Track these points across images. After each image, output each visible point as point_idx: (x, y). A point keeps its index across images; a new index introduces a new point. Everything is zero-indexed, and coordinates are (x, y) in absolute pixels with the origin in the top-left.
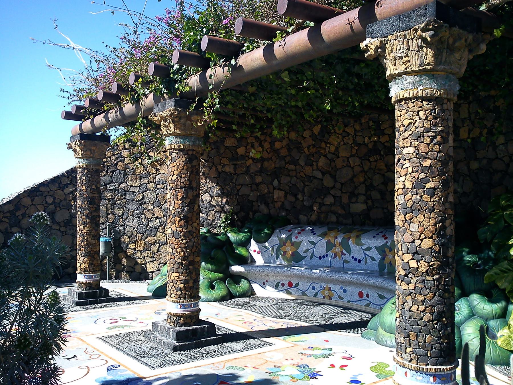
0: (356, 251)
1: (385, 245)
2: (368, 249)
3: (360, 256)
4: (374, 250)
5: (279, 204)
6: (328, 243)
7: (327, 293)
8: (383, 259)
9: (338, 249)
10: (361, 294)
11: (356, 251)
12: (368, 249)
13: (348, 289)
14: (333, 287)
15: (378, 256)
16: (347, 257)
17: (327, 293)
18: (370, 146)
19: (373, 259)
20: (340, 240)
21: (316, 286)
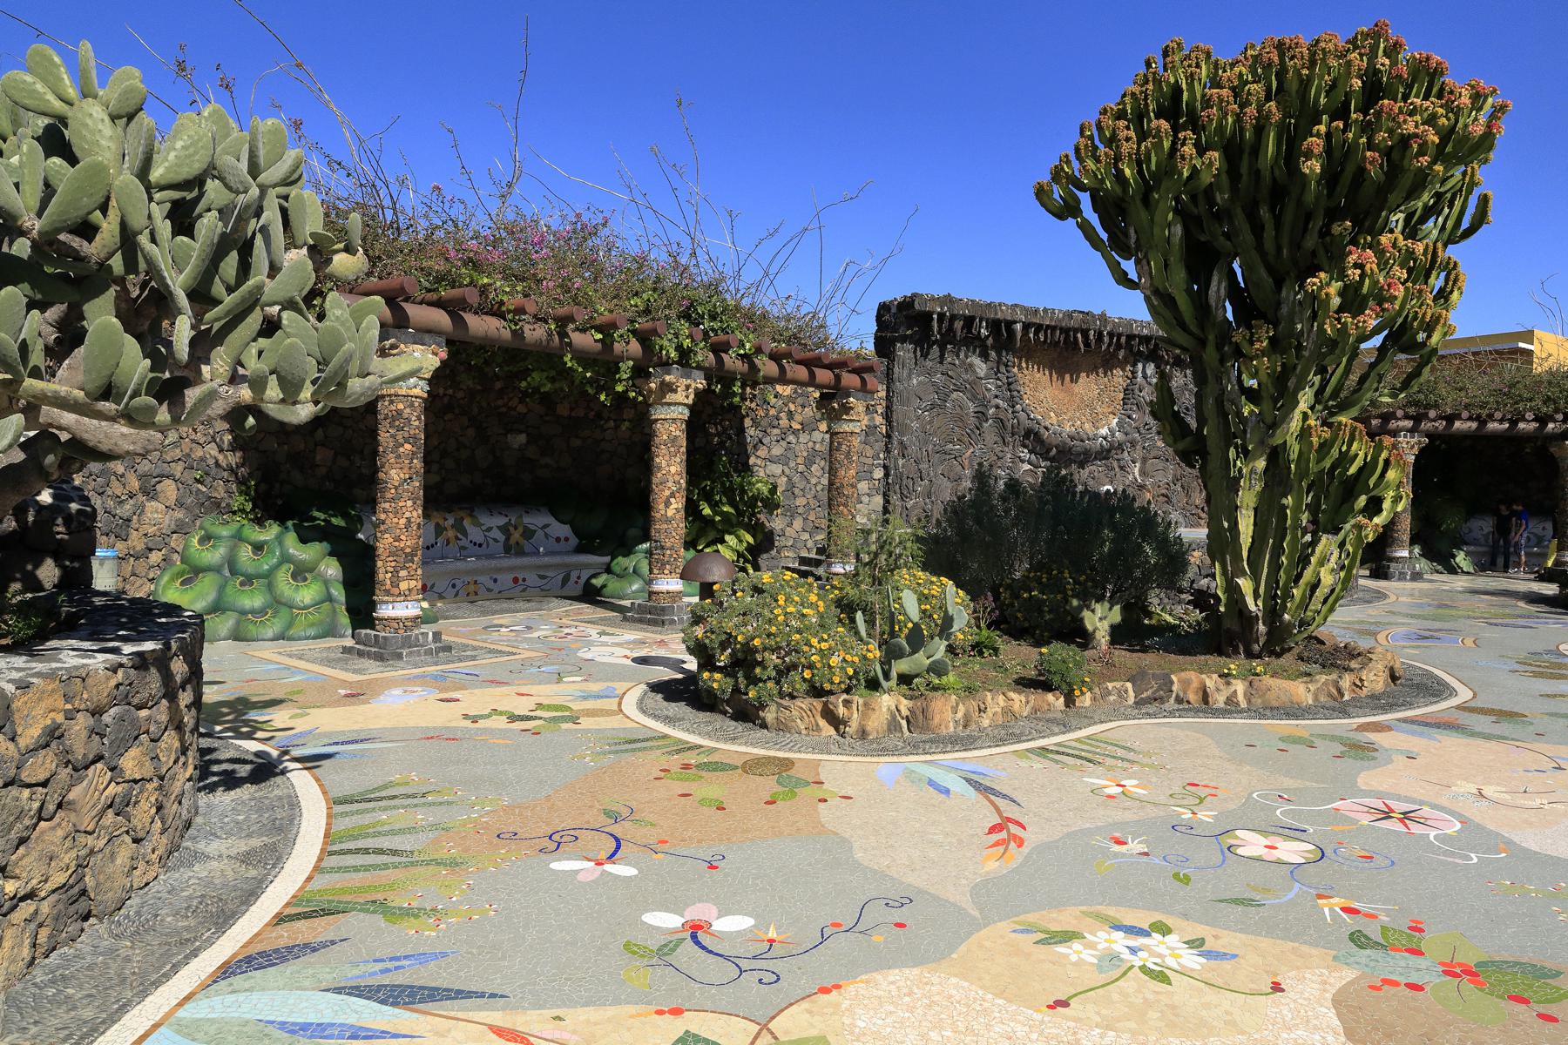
0: (475, 534)
1: (509, 523)
2: (489, 529)
3: (479, 539)
4: (495, 530)
5: (323, 470)
6: (437, 525)
7: (472, 588)
8: (508, 539)
9: (451, 533)
10: (516, 580)
11: (475, 534)
12: (489, 529)
13: (499, 577)
14: (481, 579)
15: (501, 538)
16: (464, 542)
17: (472, 588)
18: (446, 400)
19: (496, 540)
20: (451, 521)
21: (457, 582)
